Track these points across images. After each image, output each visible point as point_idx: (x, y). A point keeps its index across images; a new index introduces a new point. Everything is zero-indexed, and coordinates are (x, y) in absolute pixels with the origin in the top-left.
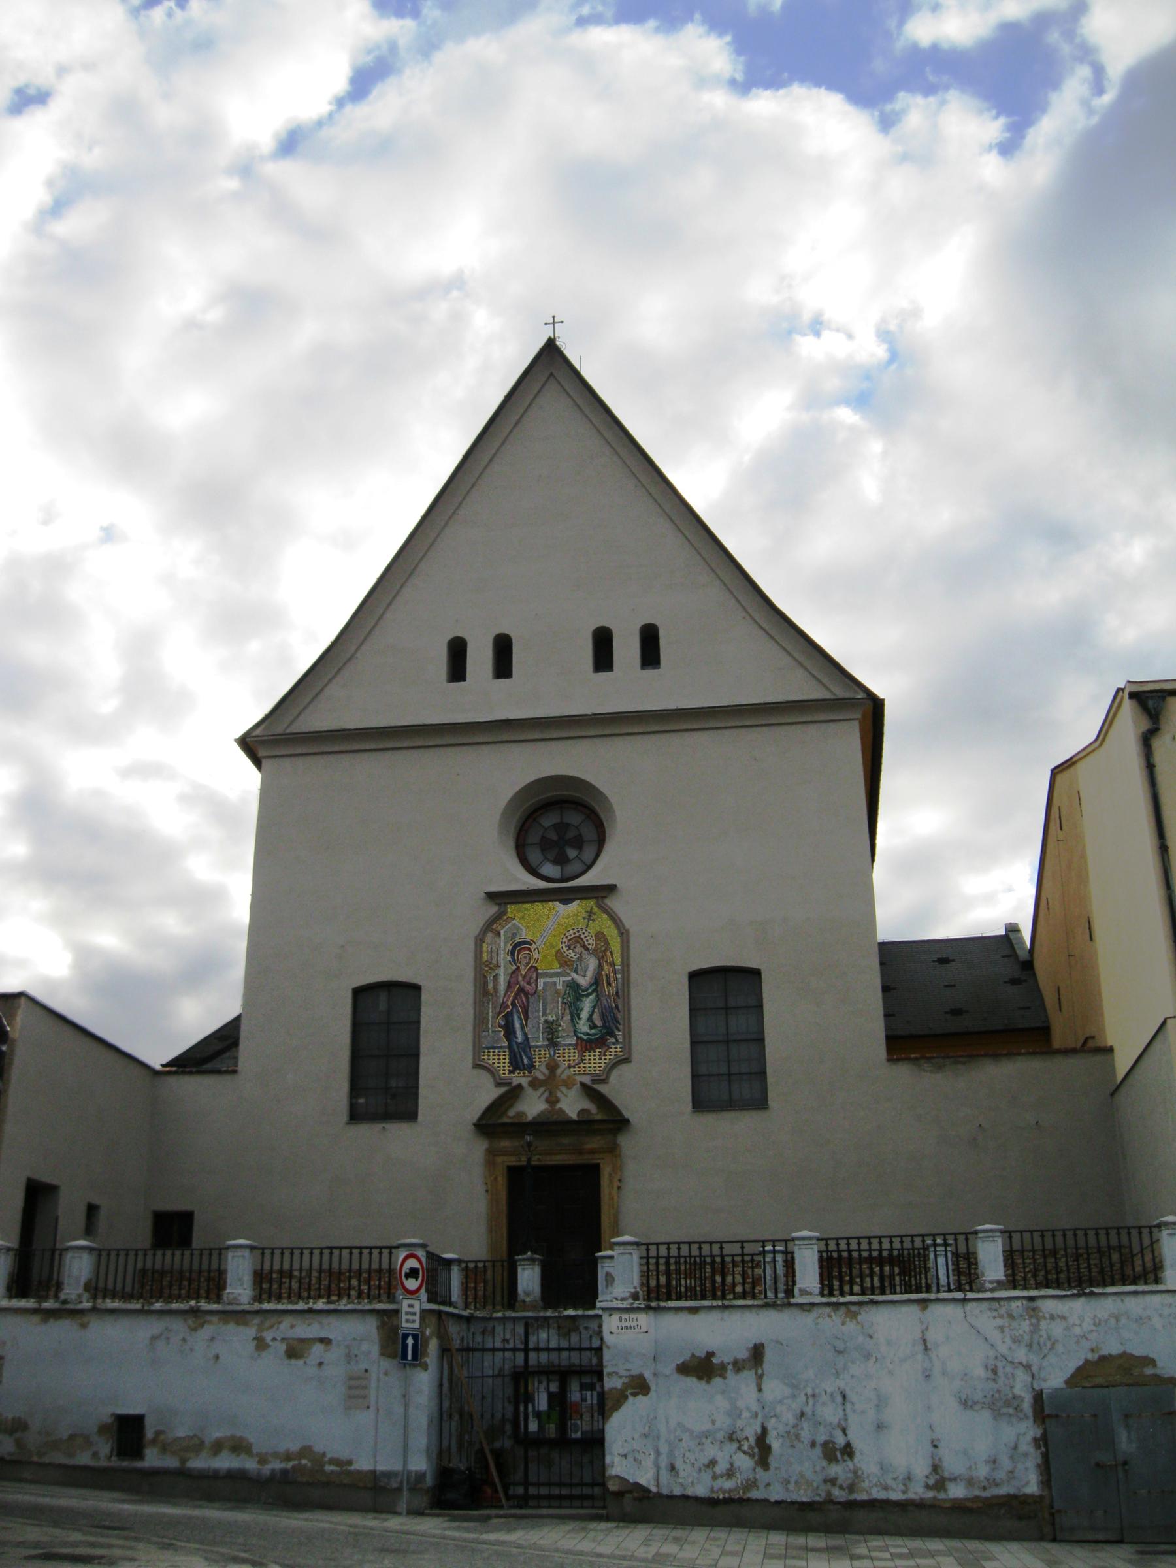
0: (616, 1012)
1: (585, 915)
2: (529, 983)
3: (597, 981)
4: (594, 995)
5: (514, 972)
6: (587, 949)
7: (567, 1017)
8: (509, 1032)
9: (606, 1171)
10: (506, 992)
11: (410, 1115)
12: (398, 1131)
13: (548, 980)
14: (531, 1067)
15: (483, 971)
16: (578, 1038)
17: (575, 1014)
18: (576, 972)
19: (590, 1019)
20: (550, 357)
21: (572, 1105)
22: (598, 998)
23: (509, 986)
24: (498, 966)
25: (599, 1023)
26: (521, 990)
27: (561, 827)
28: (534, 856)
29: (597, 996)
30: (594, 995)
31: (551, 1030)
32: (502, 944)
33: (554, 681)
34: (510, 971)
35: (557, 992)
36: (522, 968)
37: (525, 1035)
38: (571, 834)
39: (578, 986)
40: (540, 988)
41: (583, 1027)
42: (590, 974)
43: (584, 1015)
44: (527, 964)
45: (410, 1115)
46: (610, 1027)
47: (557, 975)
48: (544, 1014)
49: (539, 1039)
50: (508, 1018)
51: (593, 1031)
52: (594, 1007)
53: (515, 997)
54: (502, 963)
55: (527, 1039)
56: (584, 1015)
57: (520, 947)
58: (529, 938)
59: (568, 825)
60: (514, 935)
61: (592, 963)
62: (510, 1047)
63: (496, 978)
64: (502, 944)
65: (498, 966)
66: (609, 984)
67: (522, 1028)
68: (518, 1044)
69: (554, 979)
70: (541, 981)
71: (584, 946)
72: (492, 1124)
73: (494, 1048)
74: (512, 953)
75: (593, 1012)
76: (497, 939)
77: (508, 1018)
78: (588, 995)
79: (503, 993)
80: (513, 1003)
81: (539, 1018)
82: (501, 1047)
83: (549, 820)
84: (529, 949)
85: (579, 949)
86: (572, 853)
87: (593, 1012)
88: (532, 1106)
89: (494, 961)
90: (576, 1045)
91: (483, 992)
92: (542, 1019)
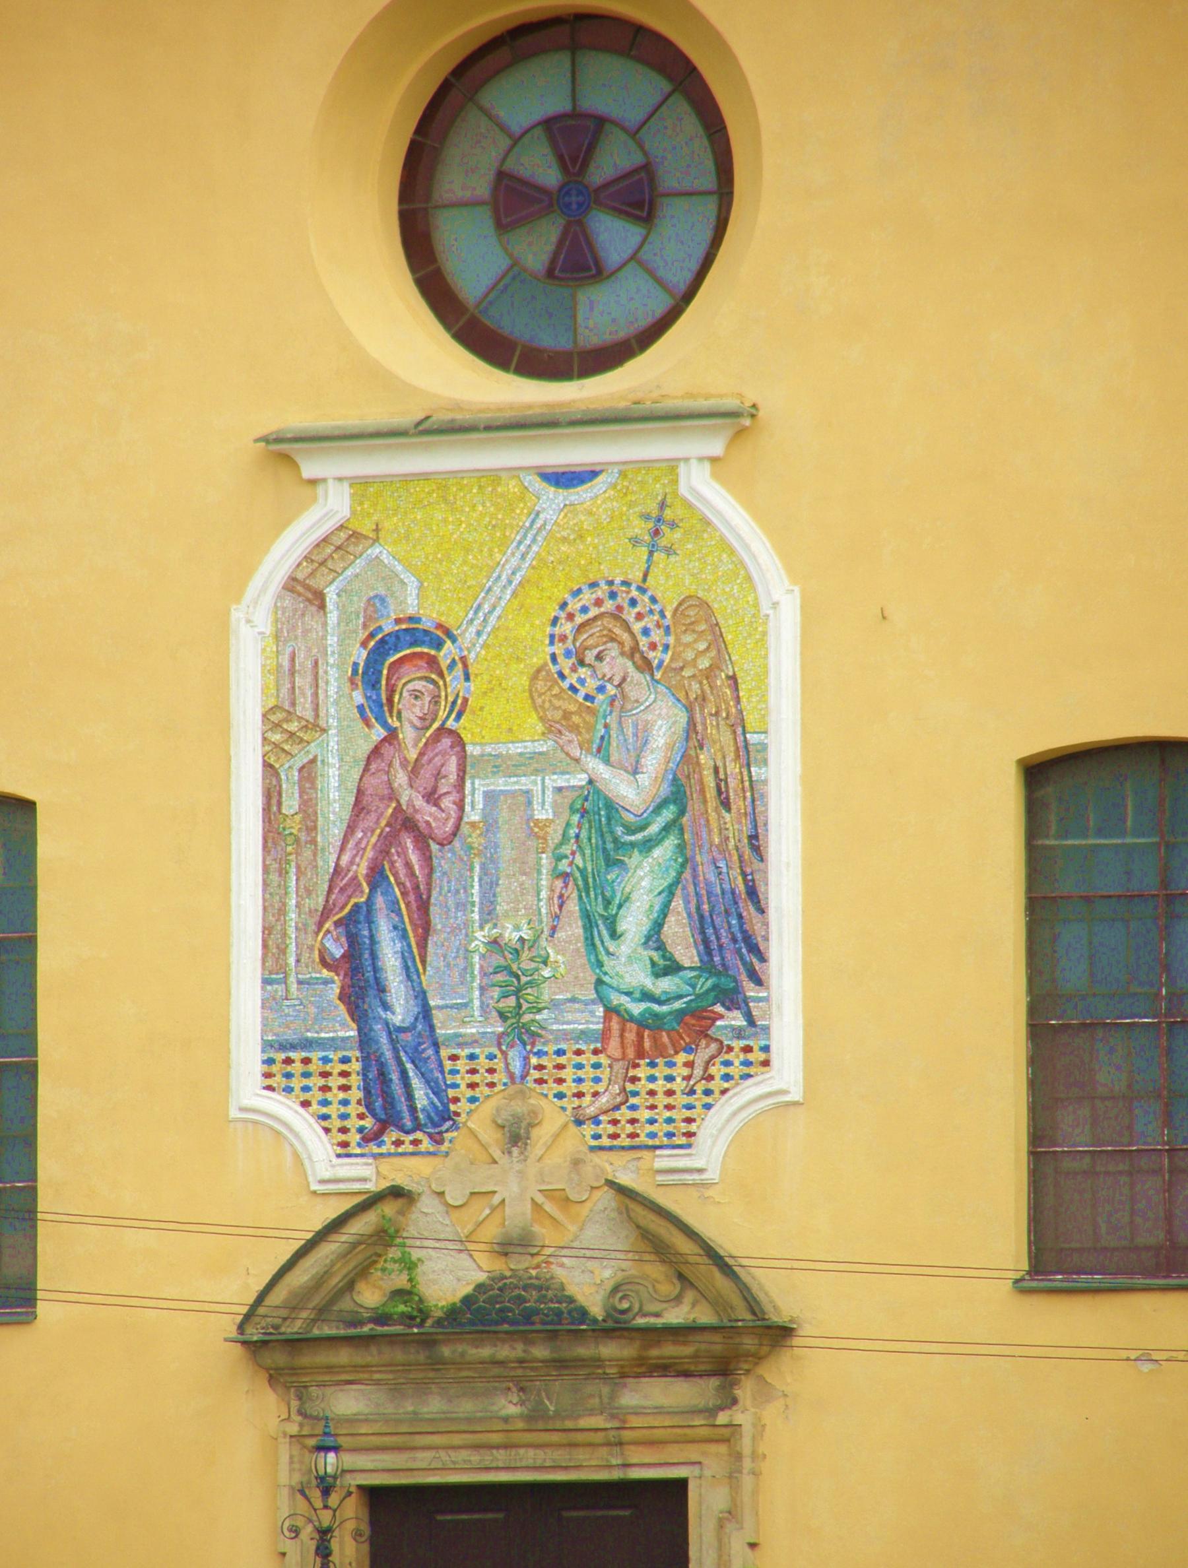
0: (749, 911)
1: (641, 528)
2: (432, 797)
3: (678, 795)
4: (671, 842)
5: (376, 752)
6: (646, 666)
7: (573, 929)
8: (359, 984)
9: (705, 1505)
10: (351, 829)
13: (501, 784)
14: (443, 1118)
16: (611, 1011)
17: (600, 924)
18: (602, 751)
19: (655, 937)
22: (686, 860)
23: (359, 808)
24: (315, 726)
25: (687, 954)
26: (405, 823)
27: (574, 135)
28: (475, 254)
29: (681, 847)
30: (671, 842)
31: (512, 975)
32: (332, 640)
34: (365, 748)
35: (535, 830)
36: (407, 734)
37: (421, 996)
38: (612, 160)
39: (611, 806)
40: (473, 815)
41: (630, 968)
42: (652, 762)
43: (634, 923)
44: (426, 720)
47: (534, 764)
48: (489, 914)
49: (467, 1019)
50: (355, 927)
51: (666, 985)
52: (670, 891)
53: (383, 852)
54: (331, 715)
55: (426, 1013)
56: (634, 923)
58: (431, 615)
59: (601, 122)
60: (376, 603)
61: (663, 724)
62: (365, 1041)
63: (309, 773)
64: (332, 640)
65: (315, 726)
66: (726, 804)
67: (410, 972)
68: (393, 1032)
69: (525, 783)
70: (477, 789)
71: (633, 652)
73: (308, 1044)
74: (370, 675)
75: (665, 911)
76: (312, 621)
77: (355, 927)
78: (648, 845)
79: (336, 832)
80: (376, 875)
81: (466, 935)
82: (333, 1044)
83: (528, 96)
84: (432, 662)
85: (616, 664)
86: (613, 235)
87: (665, 911)
89: (304, 709)
90: (605, 1035)
92: (481, 936)
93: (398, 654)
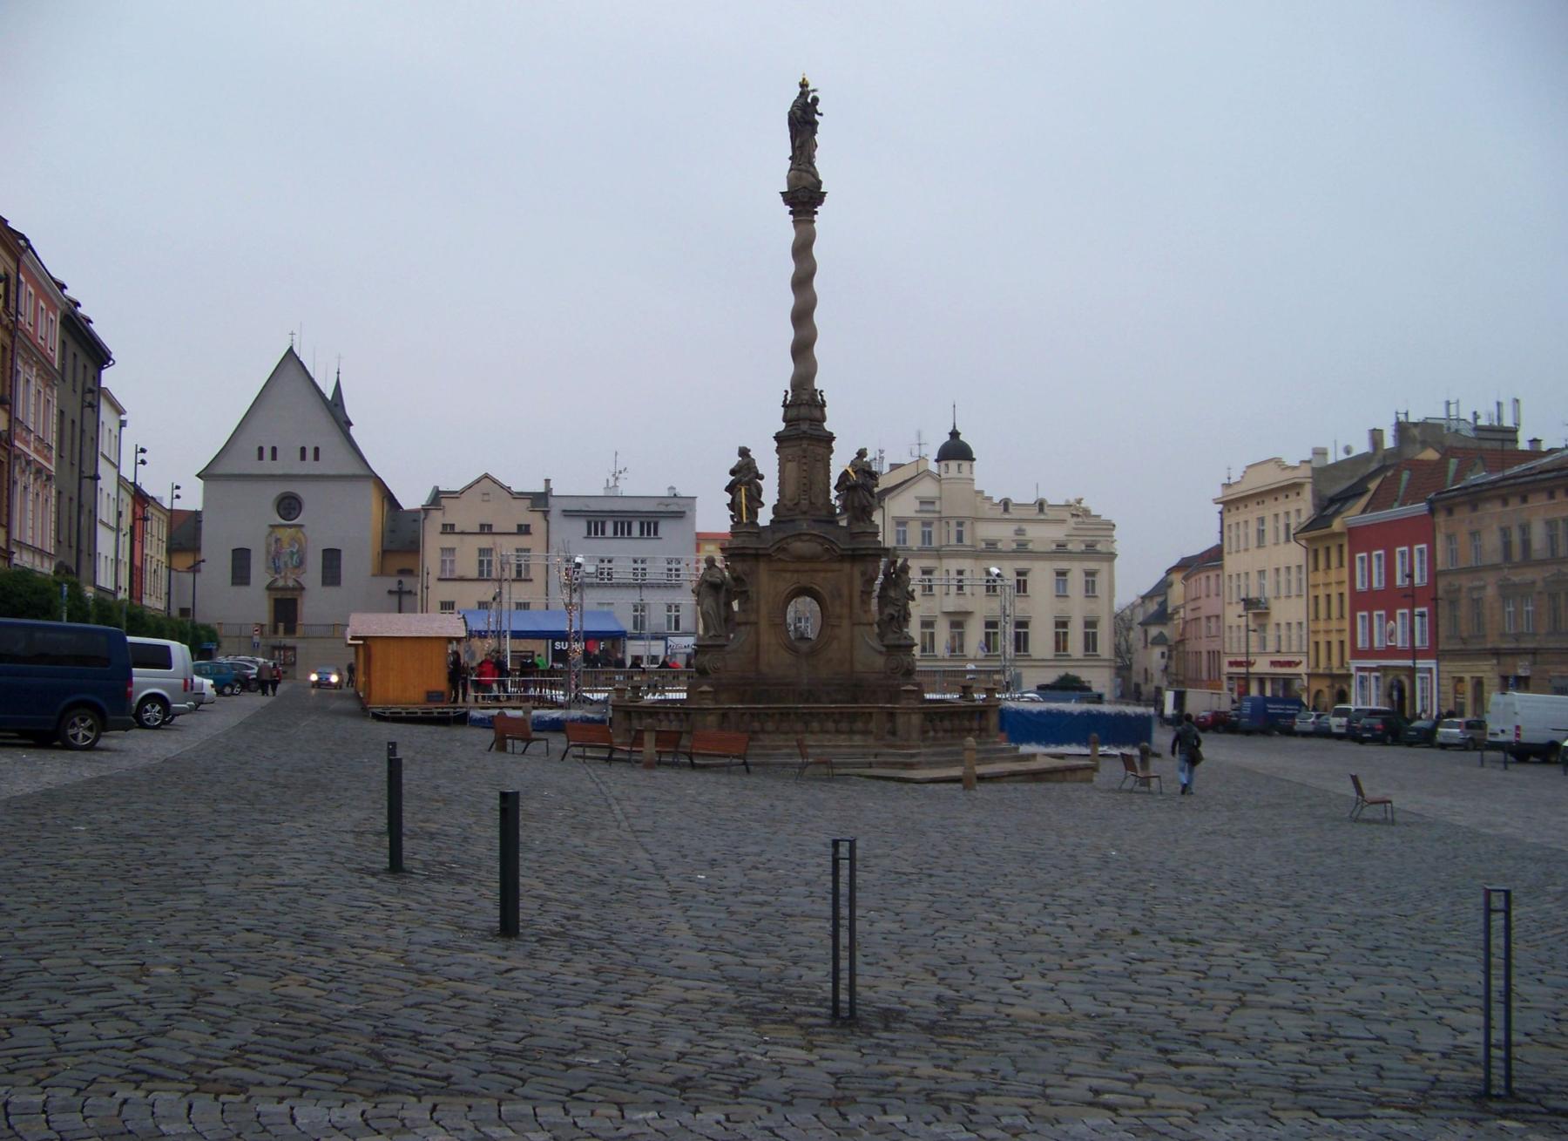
11: (248, 583)
12: (243, 589)
15: (269, 545)
20: (291, 350)
21: (291, 583)
33: (288, 463)
45: (248, 583)
46: (301, 562)
57: (278, 540)
72: (270, 588)
88: (281, 583)
91: (268, 552)
93: (278, 540)
